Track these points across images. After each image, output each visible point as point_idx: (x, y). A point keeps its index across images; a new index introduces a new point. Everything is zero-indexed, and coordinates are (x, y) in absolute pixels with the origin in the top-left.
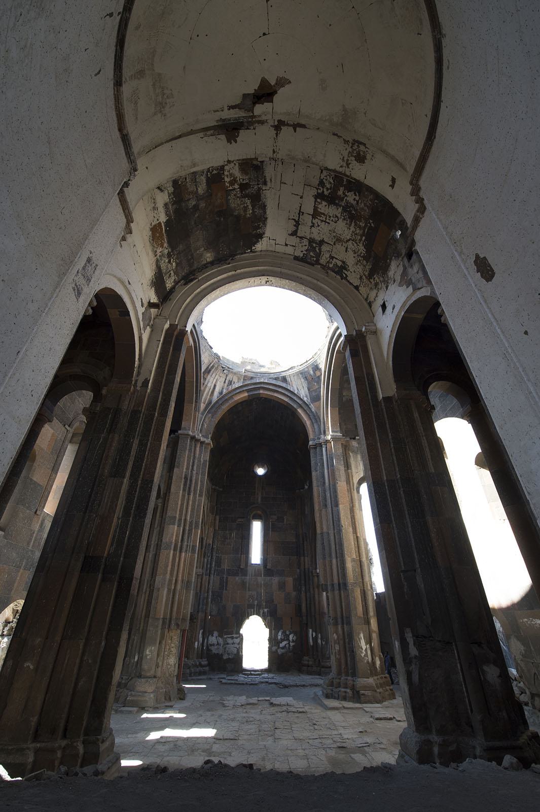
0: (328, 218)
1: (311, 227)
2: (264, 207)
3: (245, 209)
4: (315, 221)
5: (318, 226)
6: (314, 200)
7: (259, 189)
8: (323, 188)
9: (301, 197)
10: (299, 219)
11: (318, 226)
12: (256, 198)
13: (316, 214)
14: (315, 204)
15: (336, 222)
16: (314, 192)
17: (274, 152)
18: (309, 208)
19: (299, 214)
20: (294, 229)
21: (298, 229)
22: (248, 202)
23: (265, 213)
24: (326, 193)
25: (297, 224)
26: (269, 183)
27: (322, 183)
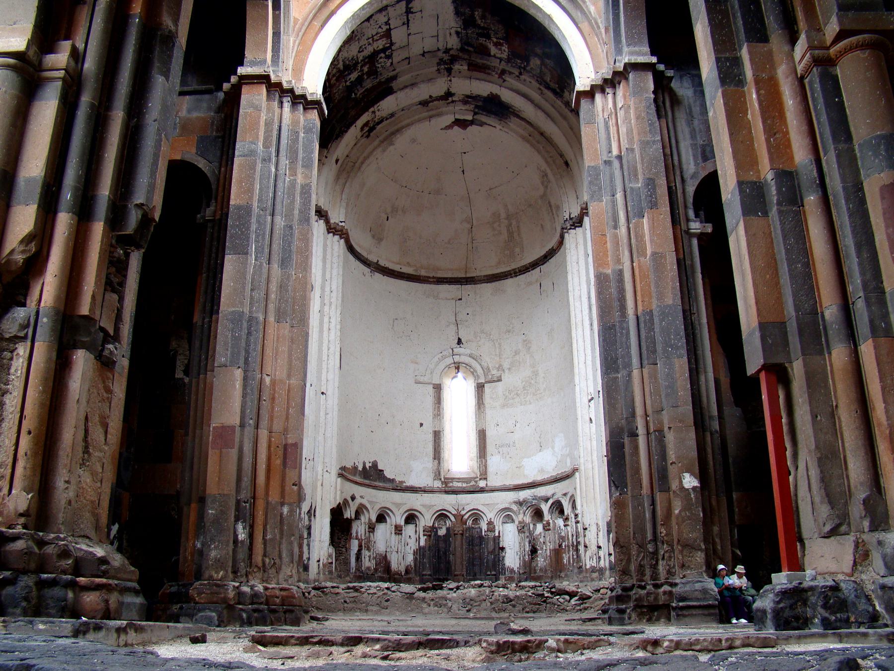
0: (371, 42)
1: (389, 20)
2: (457, 13)
3: (483, 17)
4: (385, 28)
5: (380, 27)
6: (394, 41)
7: (465, 28)
8: (386, 55)
9: (409, 35)
10: (407, 16)
11: (380, 27)
12: (468, 22)
13: (388, 34)
14: (391, 41)
15: (360, 47)
16: (393, 48)
17: (450, 81)
18: (398, 36)
19: (408, 20)
20: (410, 6)
21: (407, 7)
22: (479, 22)
23: (455, 8)
24: (383, 55)
25: (409, 11)
26: (453, 31)
27: (389, 57)
